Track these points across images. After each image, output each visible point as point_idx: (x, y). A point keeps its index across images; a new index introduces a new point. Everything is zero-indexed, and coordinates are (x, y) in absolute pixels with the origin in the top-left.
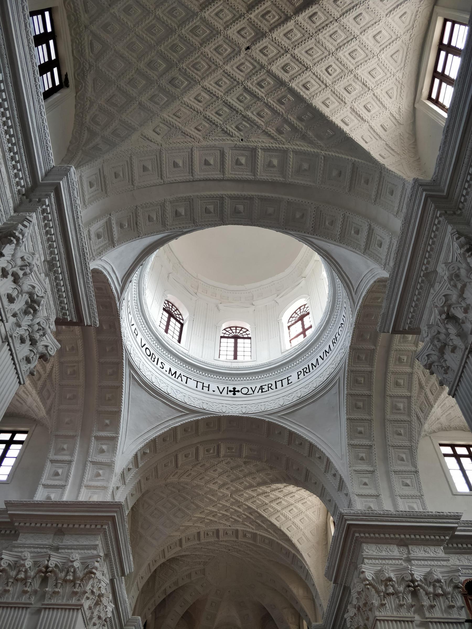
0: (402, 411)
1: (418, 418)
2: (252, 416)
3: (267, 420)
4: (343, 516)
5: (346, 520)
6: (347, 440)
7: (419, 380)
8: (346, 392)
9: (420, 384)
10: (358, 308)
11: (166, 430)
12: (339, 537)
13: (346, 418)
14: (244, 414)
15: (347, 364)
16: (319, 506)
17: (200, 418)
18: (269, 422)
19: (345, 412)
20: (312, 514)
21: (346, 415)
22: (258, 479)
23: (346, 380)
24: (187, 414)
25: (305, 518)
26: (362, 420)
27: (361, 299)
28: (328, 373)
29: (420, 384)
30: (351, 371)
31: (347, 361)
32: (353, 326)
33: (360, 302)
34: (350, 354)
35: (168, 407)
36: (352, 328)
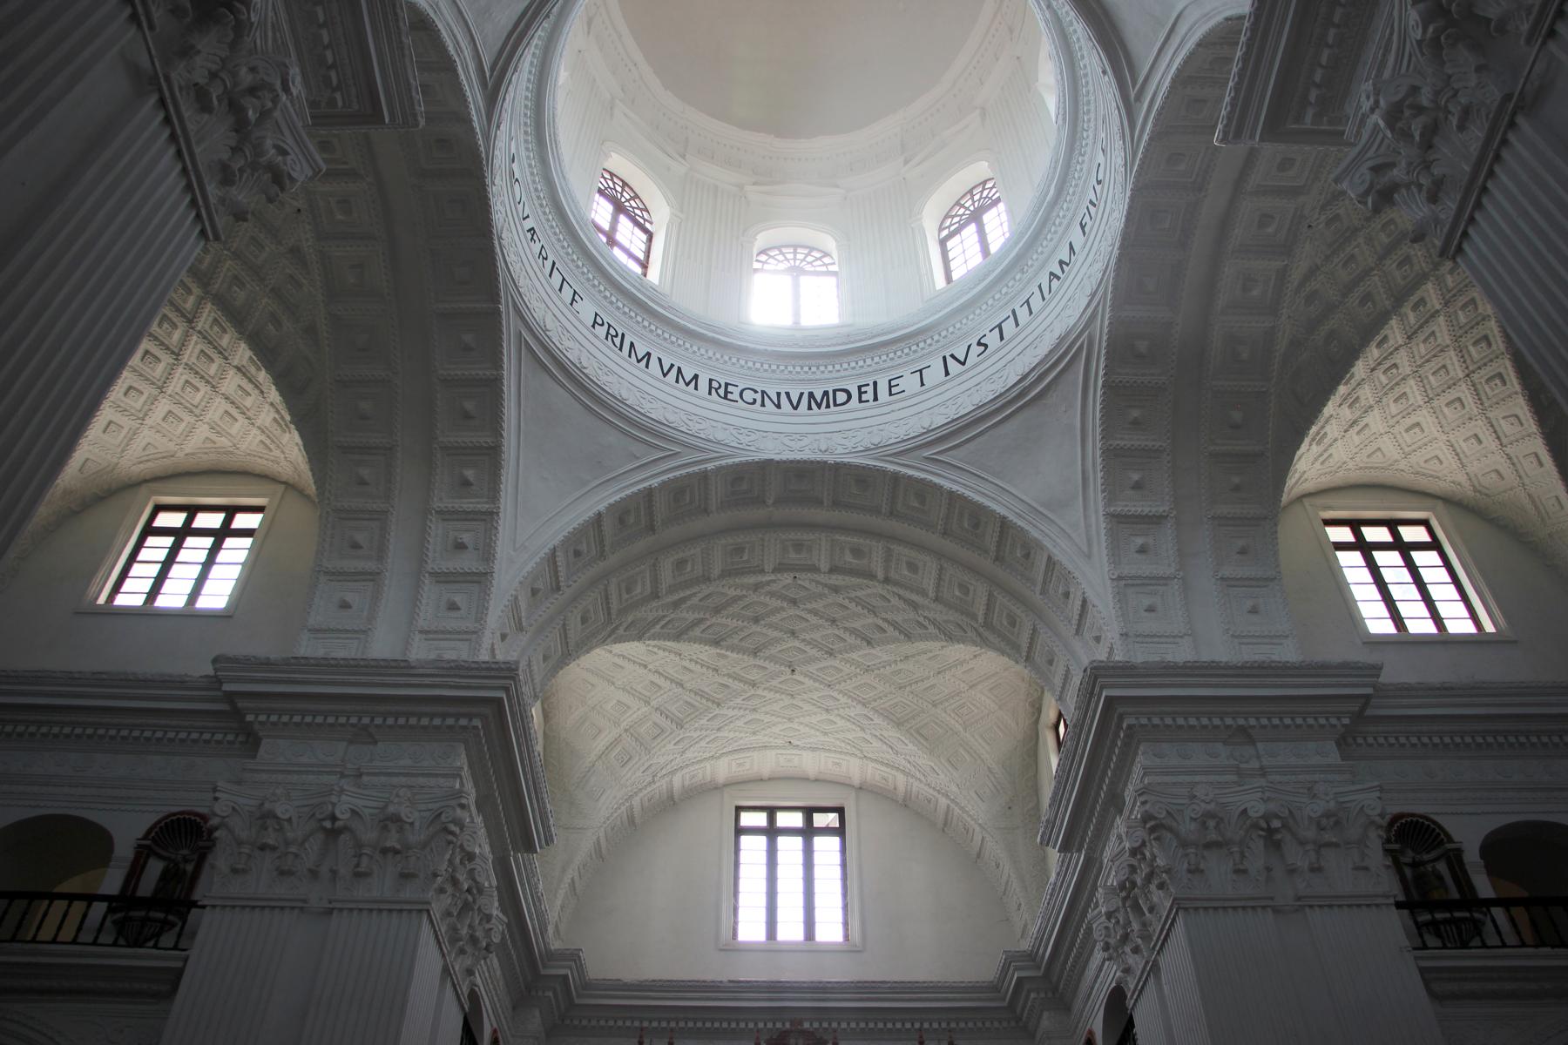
0: (625, 596)
1: (617, 628)
2: (500, 263)
3: (502, 308)
4: (513, 678)
5: (507, 689)
6: (560, 537)
7: (694, 594)
8: (655, 482)
9: (683, 600)
10: (891, 467)
11: (451, 48)
12: (427, 681)
13: (601, 507)
14: (500, 238)
15: (723, 462)
16: (180, 454)
17: (476, 124)
18: (497, 314)
19: (612, 501)
20: (143, 444)
21: (606, 504)
22: (240, 296)
23: (683, 472)
24: (484, 84)
25: (124, 432)
26: (602, 541)
27: (922, 475)
28: (671, 418)
29: (683, 600)
30: (704, 476)
31: (730, 461)
32: (831, 459)
33: (910, 472)
34: (748, 464)
35: (510, 27)
36: (825, 457)
